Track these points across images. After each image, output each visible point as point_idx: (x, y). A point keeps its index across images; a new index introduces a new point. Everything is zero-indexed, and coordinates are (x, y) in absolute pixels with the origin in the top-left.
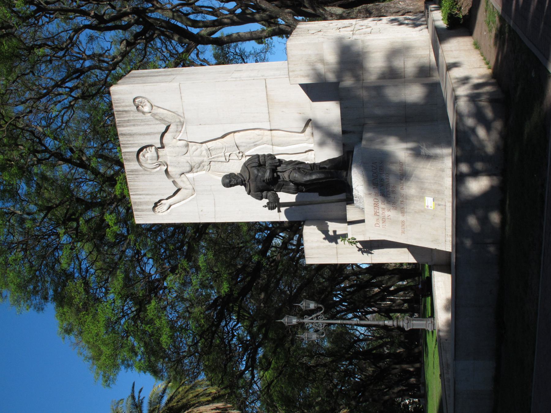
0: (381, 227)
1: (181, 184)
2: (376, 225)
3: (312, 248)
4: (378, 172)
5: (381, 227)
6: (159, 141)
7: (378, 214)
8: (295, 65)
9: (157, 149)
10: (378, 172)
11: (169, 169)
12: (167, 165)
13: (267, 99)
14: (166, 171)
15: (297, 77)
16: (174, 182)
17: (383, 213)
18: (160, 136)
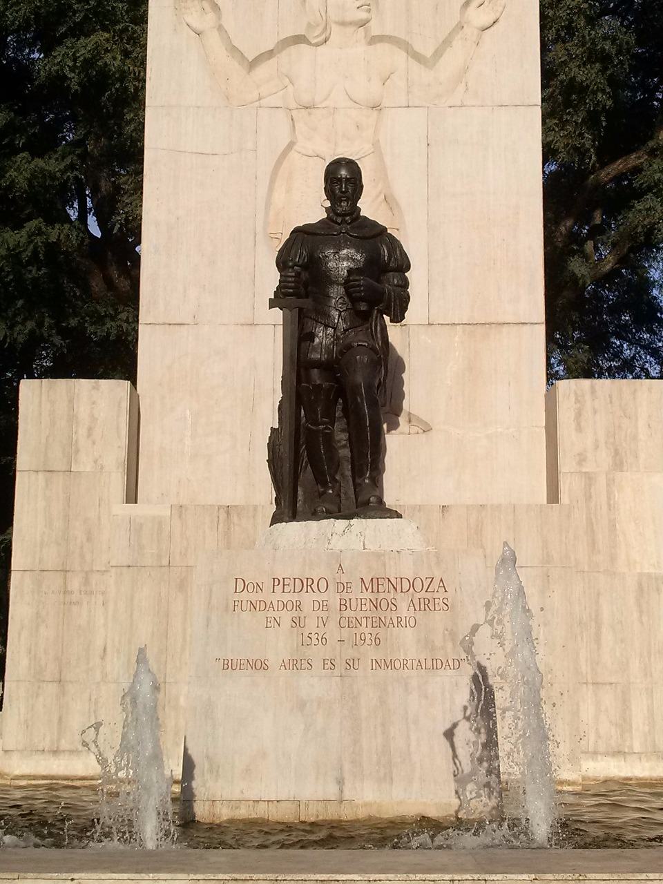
0: (237, 597)
1: (262, 71)
2: (240, 582)
3: (71, 401)
4: (419, 595)
5: (237, 597)
6: (388, 31)
7: (279, 589)
8: (610, 396)
9: (363, 24)
10: (419, 595)
11: (303, 47)
12: (317, 45)
13: (490, 324)
14: (299, 39)
15: (577, 401)
16: (270, 54)
17: (285, 606)
18: (402, 36)
